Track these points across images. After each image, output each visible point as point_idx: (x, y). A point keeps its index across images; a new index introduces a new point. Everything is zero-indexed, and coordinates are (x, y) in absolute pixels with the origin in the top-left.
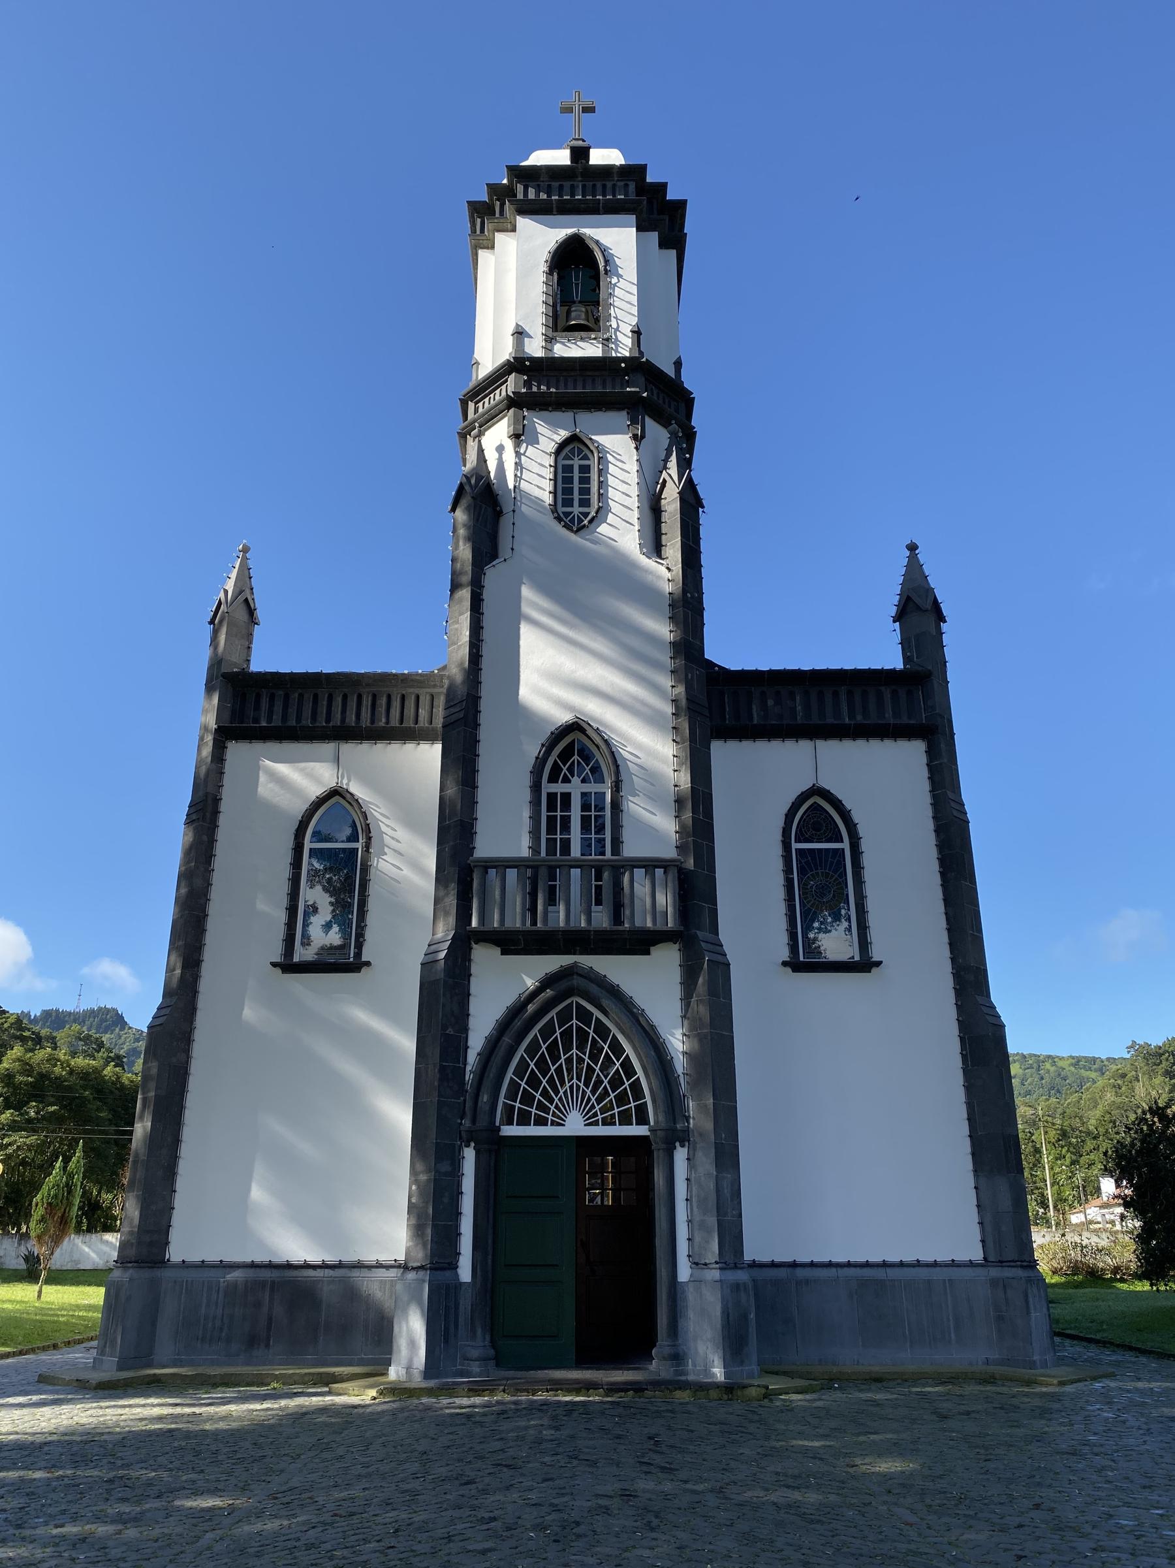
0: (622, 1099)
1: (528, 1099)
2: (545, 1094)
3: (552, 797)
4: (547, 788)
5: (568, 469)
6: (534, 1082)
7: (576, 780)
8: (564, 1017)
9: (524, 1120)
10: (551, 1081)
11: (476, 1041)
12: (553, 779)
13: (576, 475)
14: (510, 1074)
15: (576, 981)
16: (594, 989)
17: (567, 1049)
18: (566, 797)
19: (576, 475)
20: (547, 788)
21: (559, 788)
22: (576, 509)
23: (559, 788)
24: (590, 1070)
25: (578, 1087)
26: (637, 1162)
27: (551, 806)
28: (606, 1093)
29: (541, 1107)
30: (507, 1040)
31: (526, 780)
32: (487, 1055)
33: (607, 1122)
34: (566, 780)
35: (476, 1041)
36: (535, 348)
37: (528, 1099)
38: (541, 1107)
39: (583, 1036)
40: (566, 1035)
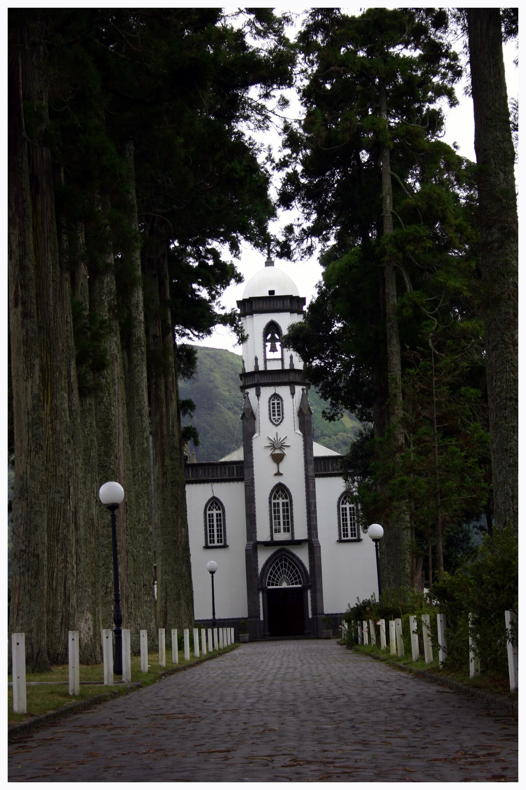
0: (295, 579)
1: (273, 580)
2: (277, 579)
3: (274, 504)
4: (273, 501)
5: (274, 404)
6: (274, 576)
7: (280, 499)
9: (273, 585)
10: (278, 576)
12: (274, 499)
13: (276, 413)
14: (269, 574)
15: (283, 552)
16: (288, 554)
17: (282, 568)
18: (278, 503)
19: (276, 413)
20: (273, 501)
21: (276, 501)
22: (277, 417)
23: (276, 501)
24: (288, 573)
25: (285, 571)
26: (300, 593)
27: (274, 506)
28: (291, 578)
29: (276, 582)
30: (268, 567)
31: (268, 501)
34: (278, 499)
36: (261, 368)
37: (273, 580)
38: (276, 582)
39: (285, 565)
40: (282, 565)
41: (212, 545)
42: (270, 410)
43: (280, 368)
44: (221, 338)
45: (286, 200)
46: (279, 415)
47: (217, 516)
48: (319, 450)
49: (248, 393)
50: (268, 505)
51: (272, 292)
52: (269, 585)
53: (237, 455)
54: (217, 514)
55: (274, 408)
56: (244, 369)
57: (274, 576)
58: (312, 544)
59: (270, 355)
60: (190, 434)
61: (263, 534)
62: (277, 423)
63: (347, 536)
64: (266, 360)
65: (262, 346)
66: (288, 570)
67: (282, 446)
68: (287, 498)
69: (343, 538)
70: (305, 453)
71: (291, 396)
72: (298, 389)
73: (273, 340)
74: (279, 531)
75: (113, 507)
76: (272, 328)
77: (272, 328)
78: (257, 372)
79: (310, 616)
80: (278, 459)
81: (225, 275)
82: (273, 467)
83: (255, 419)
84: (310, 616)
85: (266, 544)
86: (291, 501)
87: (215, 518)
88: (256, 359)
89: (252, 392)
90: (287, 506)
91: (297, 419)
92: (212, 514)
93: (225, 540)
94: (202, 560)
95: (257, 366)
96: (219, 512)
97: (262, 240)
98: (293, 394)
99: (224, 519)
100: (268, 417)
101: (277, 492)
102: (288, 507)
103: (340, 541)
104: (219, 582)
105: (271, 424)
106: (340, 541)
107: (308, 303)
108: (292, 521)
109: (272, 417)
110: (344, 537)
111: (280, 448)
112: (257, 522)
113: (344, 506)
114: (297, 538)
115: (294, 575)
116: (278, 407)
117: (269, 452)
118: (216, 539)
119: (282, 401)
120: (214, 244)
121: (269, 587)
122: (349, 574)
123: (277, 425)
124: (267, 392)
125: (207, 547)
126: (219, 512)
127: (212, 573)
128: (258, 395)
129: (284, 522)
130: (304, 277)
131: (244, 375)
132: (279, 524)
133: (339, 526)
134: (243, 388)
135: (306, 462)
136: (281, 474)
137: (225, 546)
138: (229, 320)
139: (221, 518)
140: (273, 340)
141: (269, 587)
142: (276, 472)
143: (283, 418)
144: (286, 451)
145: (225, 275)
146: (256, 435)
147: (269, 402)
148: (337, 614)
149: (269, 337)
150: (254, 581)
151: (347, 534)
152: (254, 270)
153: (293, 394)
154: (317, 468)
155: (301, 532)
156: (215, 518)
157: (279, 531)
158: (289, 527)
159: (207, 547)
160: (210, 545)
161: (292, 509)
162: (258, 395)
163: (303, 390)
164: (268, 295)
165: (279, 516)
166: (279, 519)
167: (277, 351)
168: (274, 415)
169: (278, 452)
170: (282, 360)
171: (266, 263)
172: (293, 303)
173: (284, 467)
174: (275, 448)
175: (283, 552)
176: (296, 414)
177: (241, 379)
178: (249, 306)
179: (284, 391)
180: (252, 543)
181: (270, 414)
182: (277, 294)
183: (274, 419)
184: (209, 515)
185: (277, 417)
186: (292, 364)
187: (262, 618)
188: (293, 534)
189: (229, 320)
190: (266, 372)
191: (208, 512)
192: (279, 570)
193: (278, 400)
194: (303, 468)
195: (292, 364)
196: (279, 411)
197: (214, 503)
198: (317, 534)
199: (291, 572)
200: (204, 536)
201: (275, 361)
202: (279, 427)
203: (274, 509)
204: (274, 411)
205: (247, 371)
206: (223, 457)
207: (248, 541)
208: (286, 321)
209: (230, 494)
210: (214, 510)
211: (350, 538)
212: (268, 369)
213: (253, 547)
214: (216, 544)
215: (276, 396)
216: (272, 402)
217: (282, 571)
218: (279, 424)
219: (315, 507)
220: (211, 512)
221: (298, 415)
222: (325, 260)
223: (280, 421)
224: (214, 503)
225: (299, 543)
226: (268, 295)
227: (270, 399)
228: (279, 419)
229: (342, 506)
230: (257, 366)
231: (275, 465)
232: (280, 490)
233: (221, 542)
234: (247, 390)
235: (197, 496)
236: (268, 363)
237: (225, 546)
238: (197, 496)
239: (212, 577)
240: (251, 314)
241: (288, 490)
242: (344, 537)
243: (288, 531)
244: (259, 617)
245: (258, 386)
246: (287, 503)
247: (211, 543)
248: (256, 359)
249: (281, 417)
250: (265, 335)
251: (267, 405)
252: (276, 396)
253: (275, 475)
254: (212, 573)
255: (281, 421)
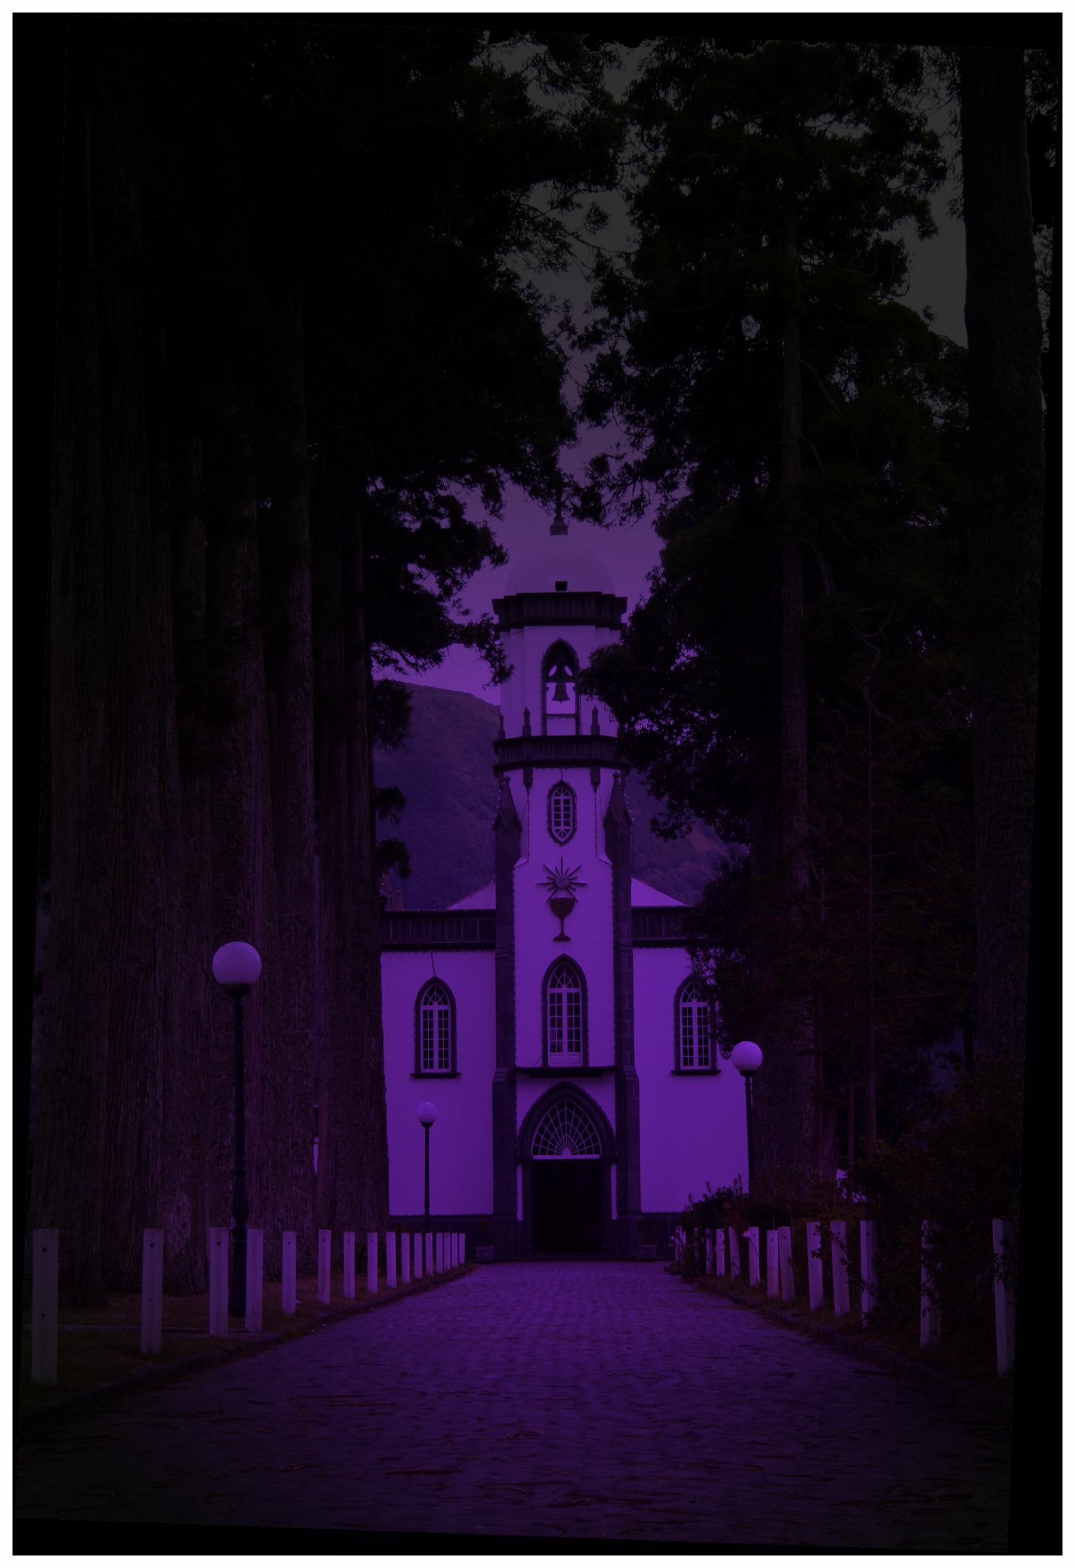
0: (588, 1143)
1: (545, 1143)
3: (552, 995)
5: (557, 802)
6: (548, 1136)
7: (564, 986)
8: (561, 1106)
9: (543, 1152)
10: (555, 1135)
11: (520, 1118)
12: (553, 986)
13: (562, 820)
14: (536, 1132)
17: (563, 1120)
18: (560, 995)
19: (562, 820)
20: (550, 991)
21: (556, 991)
22: (562, 828)
23: (556, 991)
24: (573, 1130)
25: (569, 1126)
28: (580, 1141)
29: (551, 1147)
31: (539, 989)
32: (526, 1122)
33: (582, 1153)
35: (520, 1118)
36: (536, 732)
37: (545, 1143)
38: (551, 1147)
39: (570, 1115)
40: (562, 1115)
41: (428, 1071)
42: (549, 813)
43: (573, 733)
44: (460, 671)
45: (595, 408)
46: (567, 823)
47: (440, 1016)
48: (644, 895)
49: (508, 780)
50: (540, 997)
51: (561, 585)
52: (536, 1153)
53: (483, 899)
54: (440, 1012)
55: (557, 809)
56: (502, 733)
57: (548, 1136)
58: (622, 1076)
59: (553, 707)
60: (393, 855)
61: (527, 1054)
62: (562, 840)
63: (692, 1064)
64: (545, 717)
65: (540, 689)
66: (575, 1124)
67: (570, 885)
68: (576, 986)
69: (683, 1068)
70: (616, 899)
71: (591, 788)
72: (607, 775)
73: (561, 678)
74: (560, 1050)
75: (238, 991)
76: (560, 655)
77: (560, 655)
78: (527, 739)
79: (614, 1216)
80: (562, 908)
81: (472, 548)
82: (550, 924)
83: (520, 830)
84: (614, 1216)
85: (534, 1074)
86: (585, 991)
87: (436, 1019)
88: (527, 714)
89: (516, 777)
90: (577, 1001)
91: (601, 833)
92: (431, 1012)
93: (454, 1063)
94: (406, 1100)
95: (527, 727)
96: (443, 1007)
97: (547, 484)
98: (595, 783)
99: (454, 1023)
100: (545, 826)
101: (559, 973)
102: (579, 1003)
103: (678, 1072)
104: (439, 1143)
105: (552, 840)
106: (678, 1072)
107: (631, 608)
108: (586, 1030)
109: (554, 828)
110: (685, 1064)
111: (566, 889)
112: (517, 1030)
113: (687, 1005)
114: (593, 1063)
115: (585, 1136)
116: (566, 809)
117: (546, 895)
118: (437, 1060)
119: (574, 796)
120: (453, 488)
121: (536, 1157)
122: (693, 1136)
123: (562, 844)
124: (545, 779)
125: (418, 1075)
126: (443, 1007)
127: (427, 1125)
128: (528, 783)
129: (570, 1032)
130: (626, 558)
131: (503, 744)
132: (560, 1036)
133: (677, 1044)
134: (499, 769)
135: (617, 917)
136: (567, 939)
137: (454, 1075)
138: (476, 635)
139: (448, 1020)
140: (561, 678)
141: (536, 1157)
142: (557, 934)
143: (575, 830)
144: (578, 894)
145: (472, 548)
146: (521, 861)
147: (549, 797)
148: (666, 1214)
149: (553, 671)
150: (508, 1144)
151: (691, 1060)
152: (528, 541)
153: (595, 783)
154: (639, 929)
155: (601, 1054)
156: (436, 1019)
157: (560, 1050)
158: (579, 1041)
159: (418, 1075)
160: (423, 1071)
161: (585, 1007)
162: (528, 783)
163: (615, 776)
164: (554, 590)
165: (560, 1021)
166: (560, 1025)
167: (567, 699)
168: (558, 824)
169: (562, 895)
170: (577, 716)
171: (552, 527)
172: (601, 608)
173: (572, 924)
174: (558, 888)
175: (565, 1090)
176: (600, 823)
177: (496, 752)
178: (517, 611)
179: (578, 778)
180: (506, 1069)
181: (549, 821)
182: (570, 589)
183: (557, 831)
184: (425, 1012)
185: (562, 828)
186: (595, 726)
187: (520, 1217)
188: (586, 1055)
189: (476, 635)
190: (545, 740)
191: (423, 1008)
192: (557, 1125)
193: (567, 795)
194: (611, 928)
195: (595, 726)
196: (567, 816)
197: (436, 989)
198: (633, 1056)
199: (580, 1130)
200: (413, 1054)
201: (563, 719)
202: (566, 846)
203: (550, 1006)
204: (558, 816)
205: (507, 737)
206: (455, 901)
207: (498, 1066)
208: (587, 642)
209: (467, 973)
210: (435, 1003)
211: (696, 1066)
212: (549, 734)
213: (508, 1078)
214: (436, 1069)
215: (562, 787)
216: (554, 797)
217: (563, 1127)
218: (566, 842)
219: (631, 1005)
220: (428, 1008)
221: (605, 826)
222: (666, 526)
223: (568, 835)
224: (436, 989)
225: (598, 1073)
226: (554, 590)
227: (551, 791)
228: (568, 831)
229: (682, 1005)
230: (527, 727)
231: (557, 921)
232: (565, 969)
233: (447, 1067)
234: (506, 774)
235: (402, 975)
236: (549, 721)
237: (454, 1075)
238: (402, 975)
239: (427, 1133)
240: (520, 625)
241: (578, 969)
242: (685, 1064)
243: (577, 1050)
244: (514, 1213)
245: (528, 766)
246: (577, 995)
247: (426, 1067)
248: (527, 714)
249: (570, 828)
250: (546, 668)
251: (546, 803)
252: (562, 787)
253: (556, 939)
254: (427, 1125)
255: (571, 837)
